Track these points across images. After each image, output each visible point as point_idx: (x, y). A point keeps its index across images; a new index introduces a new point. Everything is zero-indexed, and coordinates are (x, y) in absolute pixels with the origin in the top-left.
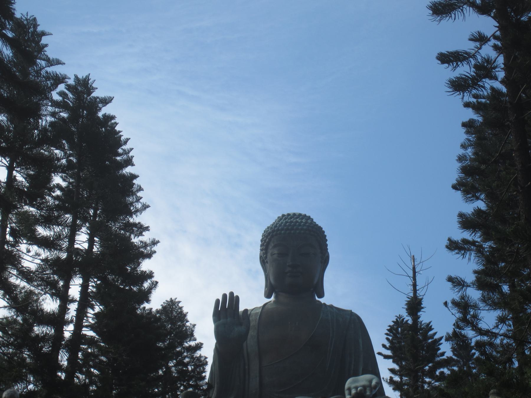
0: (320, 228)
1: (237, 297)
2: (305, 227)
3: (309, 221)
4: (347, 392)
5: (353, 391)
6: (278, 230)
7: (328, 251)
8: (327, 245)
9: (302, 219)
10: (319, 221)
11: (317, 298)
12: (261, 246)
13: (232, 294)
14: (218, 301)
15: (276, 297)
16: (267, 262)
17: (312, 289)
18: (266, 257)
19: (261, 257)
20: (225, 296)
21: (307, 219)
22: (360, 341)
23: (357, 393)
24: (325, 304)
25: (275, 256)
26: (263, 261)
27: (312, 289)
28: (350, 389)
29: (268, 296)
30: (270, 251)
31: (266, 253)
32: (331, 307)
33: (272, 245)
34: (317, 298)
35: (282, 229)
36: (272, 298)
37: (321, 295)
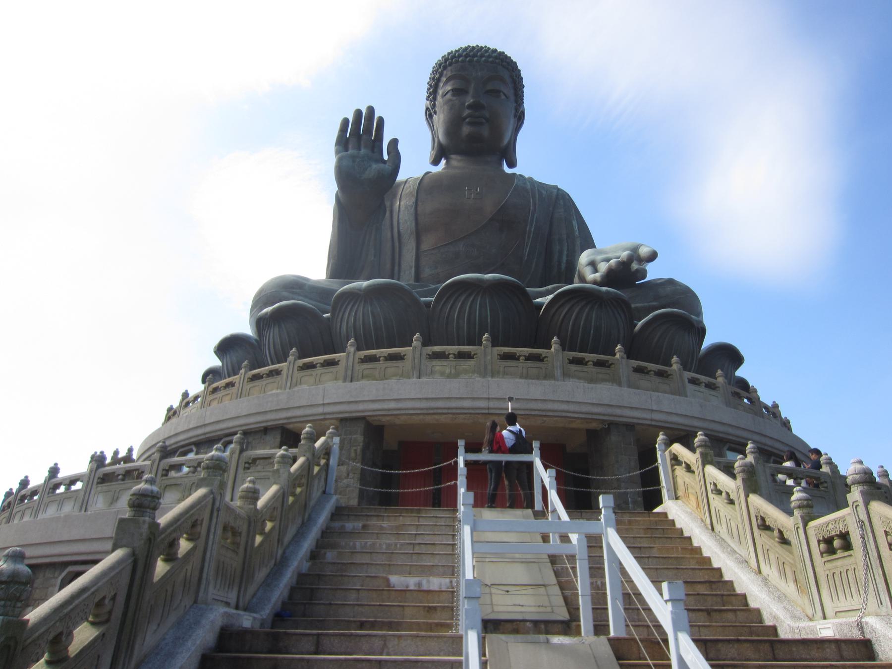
1: (381, 121)
12: (428, 89)
13: (371, 110)
14: (345, 122)
15: (447, 163)
16: (435, 113)
18: (434, 105)
19: (427, 109)
20: (358, 113)
22: (575, 223)
25: (449, 96)
26: (429, 115)
28: (593, 264)
29: (436, 162)
30: (440, 92)
31: (435, 99)
33: (444, 79)
37: (512, 164)
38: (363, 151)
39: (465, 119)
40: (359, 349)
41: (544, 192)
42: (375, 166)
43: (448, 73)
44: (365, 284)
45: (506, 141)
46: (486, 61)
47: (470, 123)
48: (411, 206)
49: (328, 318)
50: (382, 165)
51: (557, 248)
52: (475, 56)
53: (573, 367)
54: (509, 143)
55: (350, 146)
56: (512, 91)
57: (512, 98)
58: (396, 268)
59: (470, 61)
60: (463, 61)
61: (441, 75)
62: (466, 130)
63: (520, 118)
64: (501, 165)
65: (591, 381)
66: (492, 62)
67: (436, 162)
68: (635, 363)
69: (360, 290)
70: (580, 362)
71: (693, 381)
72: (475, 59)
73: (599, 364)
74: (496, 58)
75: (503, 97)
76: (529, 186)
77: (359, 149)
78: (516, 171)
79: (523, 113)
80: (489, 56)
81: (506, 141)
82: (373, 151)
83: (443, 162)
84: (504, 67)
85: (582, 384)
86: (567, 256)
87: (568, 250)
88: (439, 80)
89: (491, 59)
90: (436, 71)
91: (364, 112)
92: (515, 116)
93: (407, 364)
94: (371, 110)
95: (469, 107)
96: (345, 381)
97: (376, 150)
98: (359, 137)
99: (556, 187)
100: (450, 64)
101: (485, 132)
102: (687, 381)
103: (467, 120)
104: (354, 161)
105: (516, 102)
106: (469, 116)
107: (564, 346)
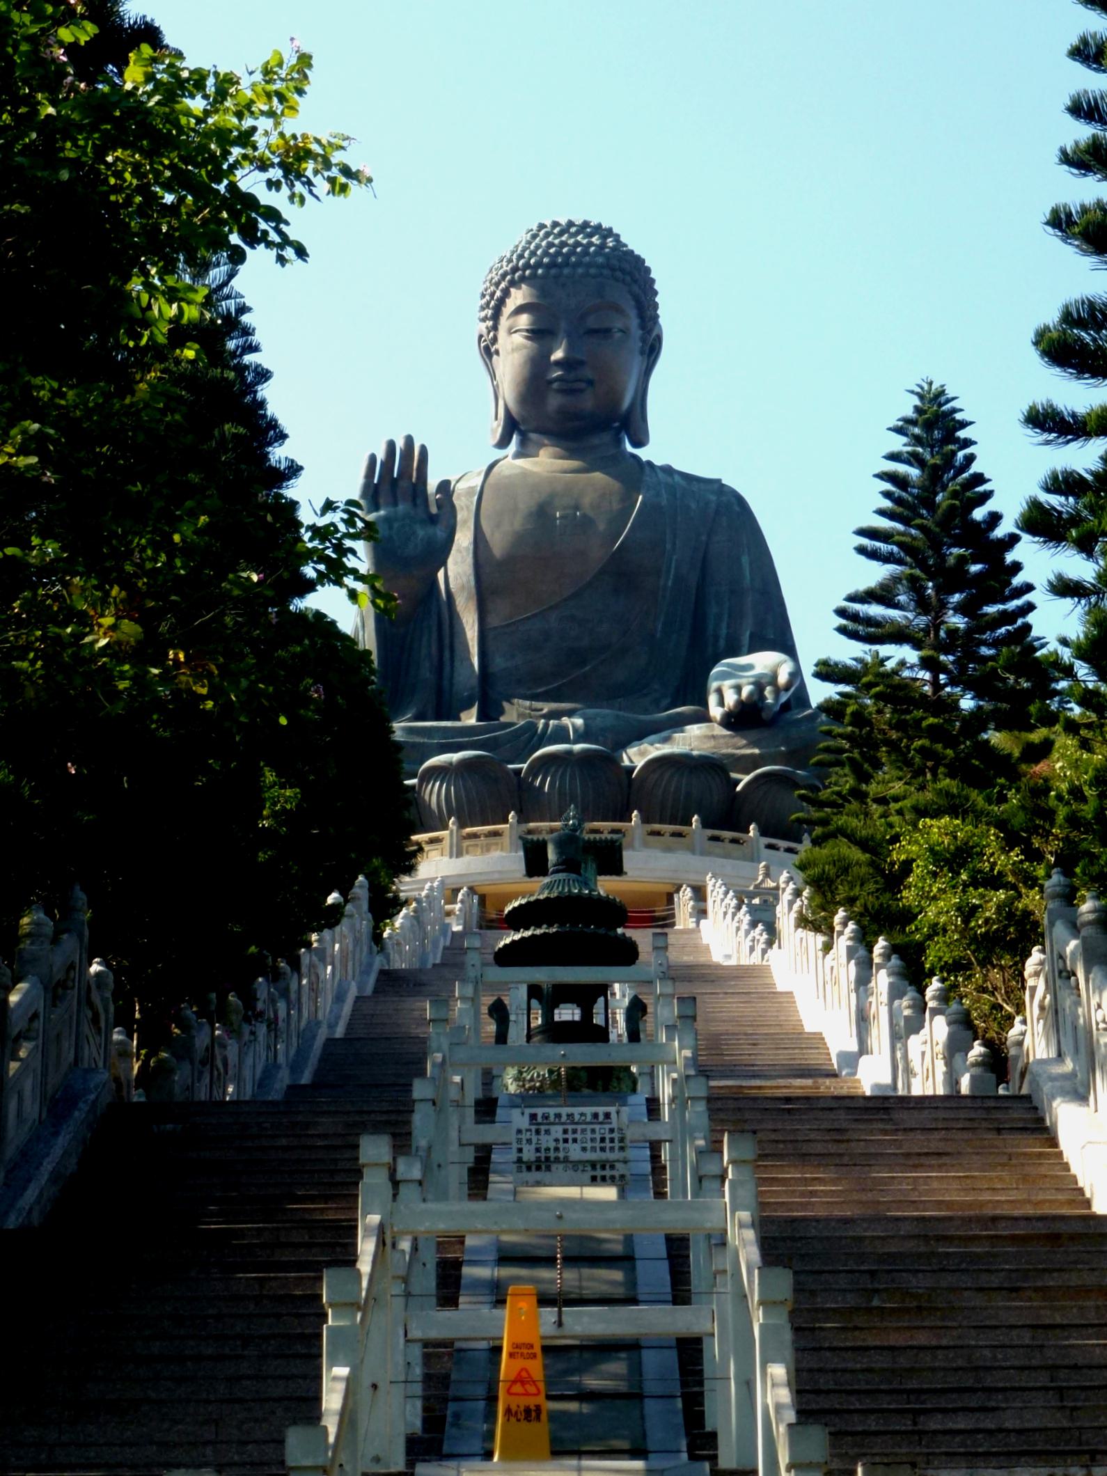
0: (639, 261)
1: (424, 450)
2: (600, 260)
3: (610, 242)
4: (712, 699)
5: (731, 699)
6: (527, 266)
7: (661, 320)
8: (656, 306)
9: (591, 235)
10: (635, 242)
11: (629, 448)
13: (409, 441)
14: (373, 459)
16: (497, 352)
17: (617, 424)
18: (495, 340)
20: (391, 446)
21: (604, 238)
22: (745, 560)
23: (740, 703)
24: (649, 463)
26: (488, 352)
27: (617, 424)
29: (503, 443)
30: (504, 322)
31: (495, 328)
32: (668, 470)
34: (629, 448)
35: (539, 264)
36: (513, 447)
37: (640, 440)
38: (402, 508)
39: (551, 382)
40: (462, 825)
41: (693, 506)
42: (421, 533)
43: (519, 297)
44: (455, 757)
45: (626, 403)
46: (586, 275)
47: (559, 391)
48: (467, 549)
49: (413, 787)
50: (430, 530)
51: (713, 610)
52: (566, 263)
53: (651, 838)
54: (632, 405)
55: (381, 501)
56: (632, 313)
57: (634, 322)
58: (447, 654)
59: (556, 277)
60: (543, 277)
61: (506, 293)
62: (554, 402)
63: (652, 349)
64: (619, 442)
65: (668, 849)
66: (594, 277)
67: (503, 443)
68: (710, 832)
69: (451, 764)
70: (658, 833)
71: (770, 847)
72: (566, 271)
73: (674, 834)
74: (602, 266)
75: (619, 335)
76: (664, 500)
77: (395, 504)
78: (643, 454)
79: (659, 339)
80: (589, 265)
81: (626, 403)
82: (415, 505)
83: (515, 438)
84: (617, 280)
85: (660, 854)
86: (729, 627)
87: (730, 616)
88: (501, 302)
89: (593, 271)
90: (497, 284)
91: (400, 444)
92: (642, 353)
93: (506, 840)
94: (409, 441)
95: (558, 363)
96: (451, 857)
97: (419, 501)
98: (394, 482)
99: (716, 486)
100: (523, 279)
101: (588, 402)
102: (762, 846)
103: (555, 385)
104: (391, 528)
105: (643, 326)
106: (557, 379)
107: (646, 820)
